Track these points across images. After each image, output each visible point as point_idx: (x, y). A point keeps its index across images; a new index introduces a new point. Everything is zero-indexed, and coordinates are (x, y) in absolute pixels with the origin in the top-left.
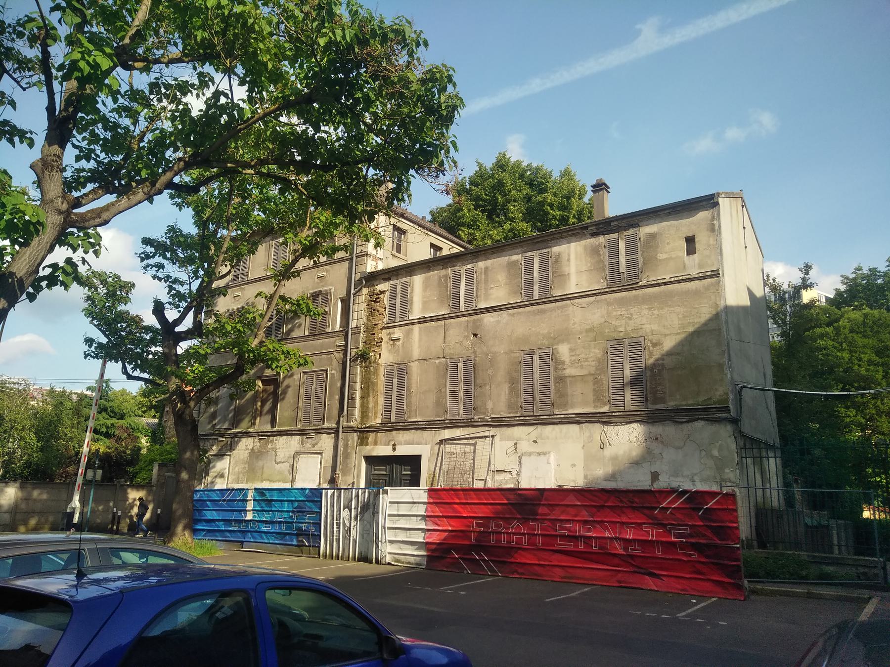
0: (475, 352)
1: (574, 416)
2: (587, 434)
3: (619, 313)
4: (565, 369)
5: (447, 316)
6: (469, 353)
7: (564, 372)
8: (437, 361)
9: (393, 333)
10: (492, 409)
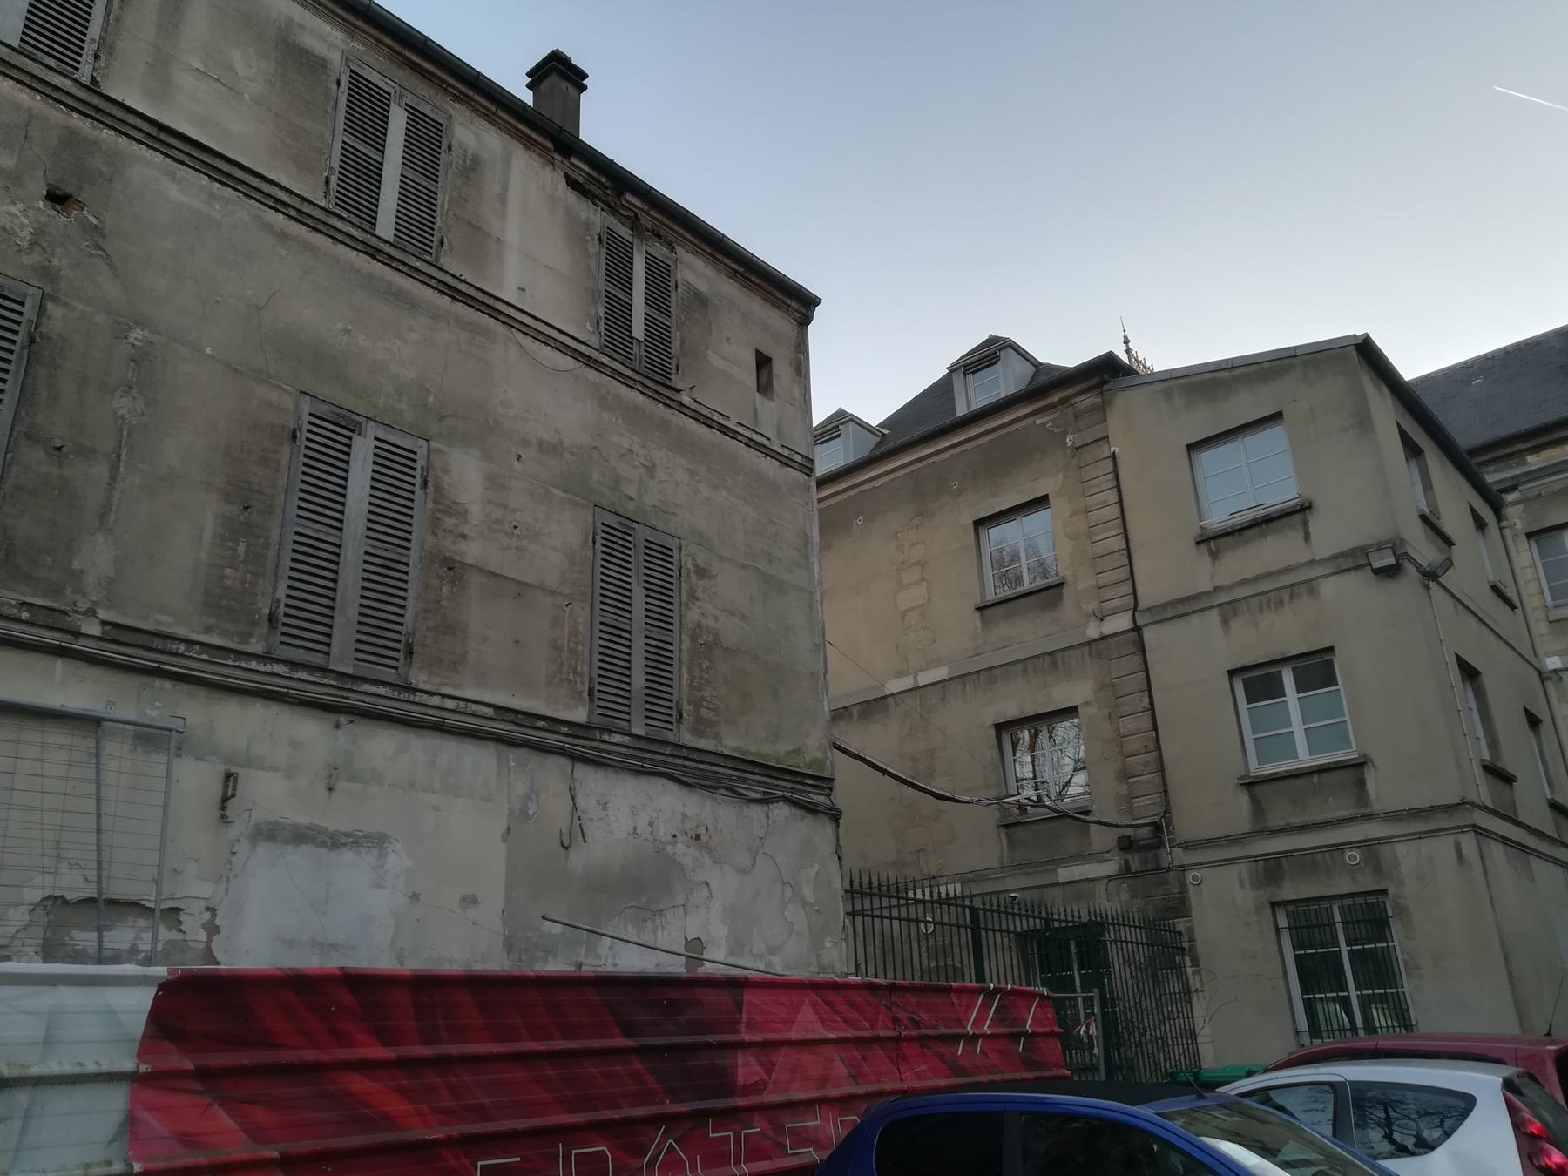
1: (489, 712)
2: (520, 787)
3: (625, 443)
4: (464, 536)
7: (463, 546)
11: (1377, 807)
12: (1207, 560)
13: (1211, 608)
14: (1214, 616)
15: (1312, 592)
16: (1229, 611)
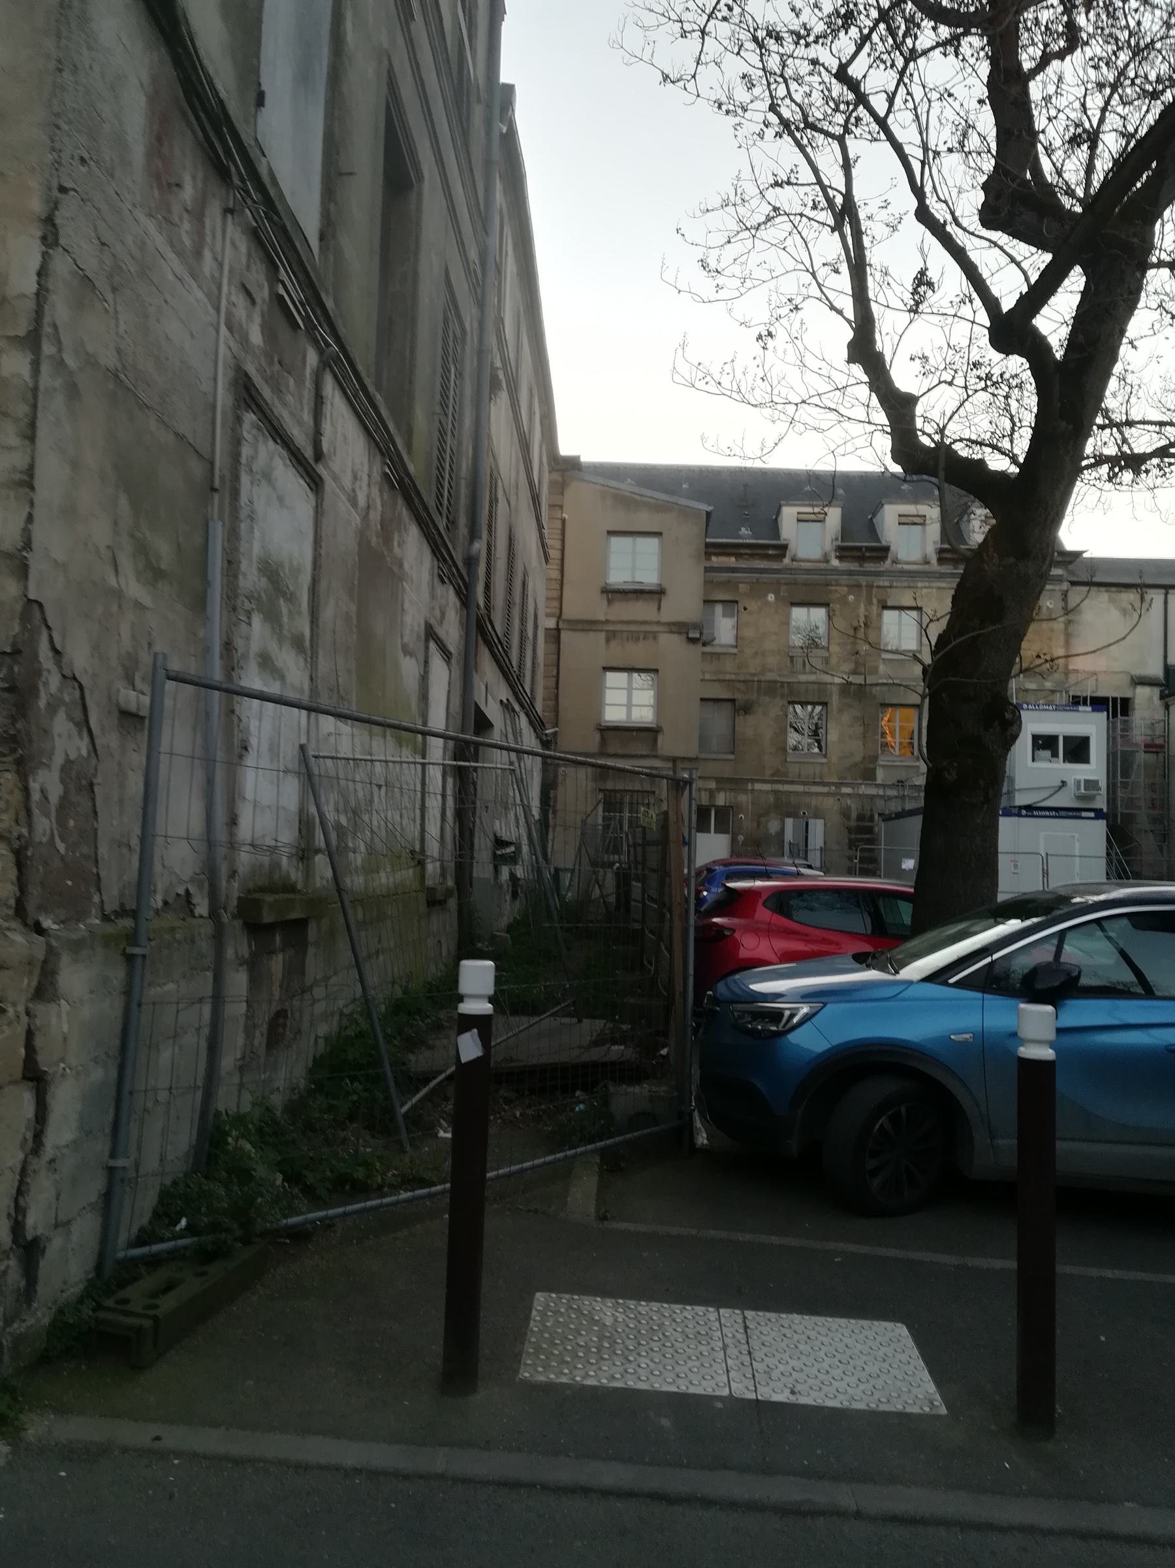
11: (660, 752)
12: (606, 602)
13: (602, 631)
14: (602, 635)
15: (655, 638)
16: (611, 636)
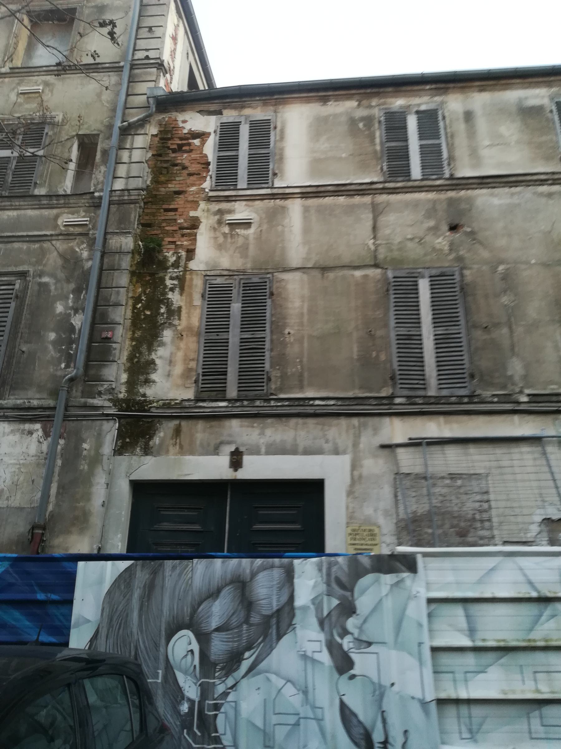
0: (460, 259)
5: (380, 186)
6: (447, 263)
8: (358, 274)
9: (230, 212)
10: (525, 377)
